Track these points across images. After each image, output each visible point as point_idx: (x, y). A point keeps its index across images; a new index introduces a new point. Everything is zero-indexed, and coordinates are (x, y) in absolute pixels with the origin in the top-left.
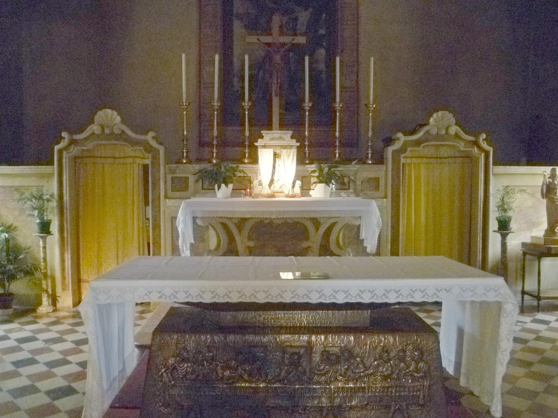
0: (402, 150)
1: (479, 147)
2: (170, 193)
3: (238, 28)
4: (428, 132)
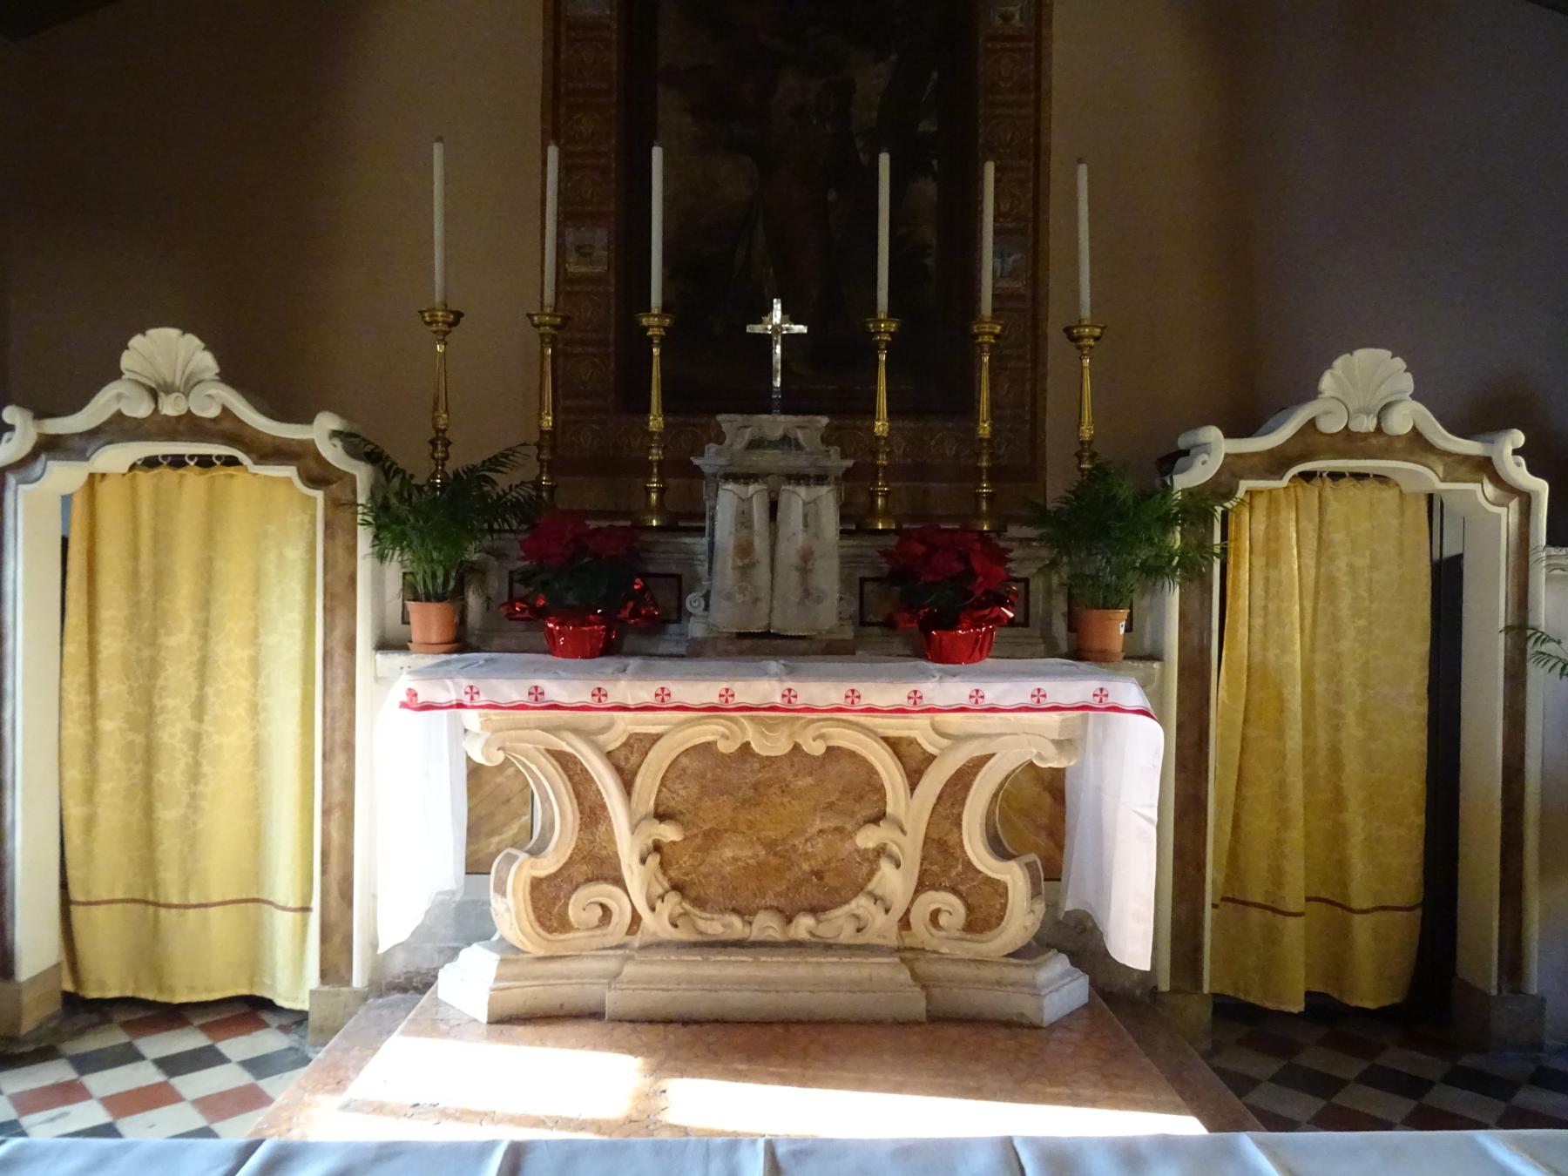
1: (1497, 480)
4: (1312, 423)
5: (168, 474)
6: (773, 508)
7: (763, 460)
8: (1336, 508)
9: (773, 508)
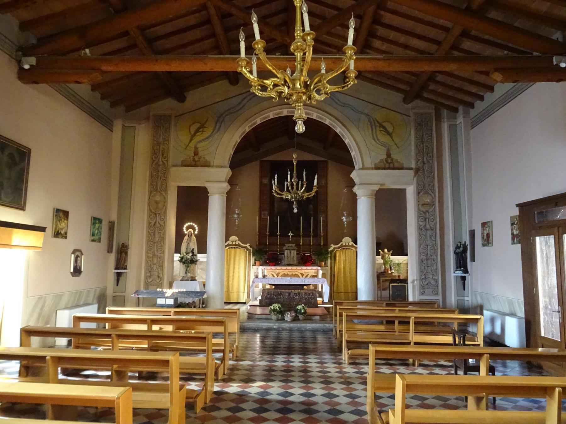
4: (342, 244)
5: (231, 249)
6: (290, 253)
7: (289, 248)
8: (347, 252)
9: (290, 253)
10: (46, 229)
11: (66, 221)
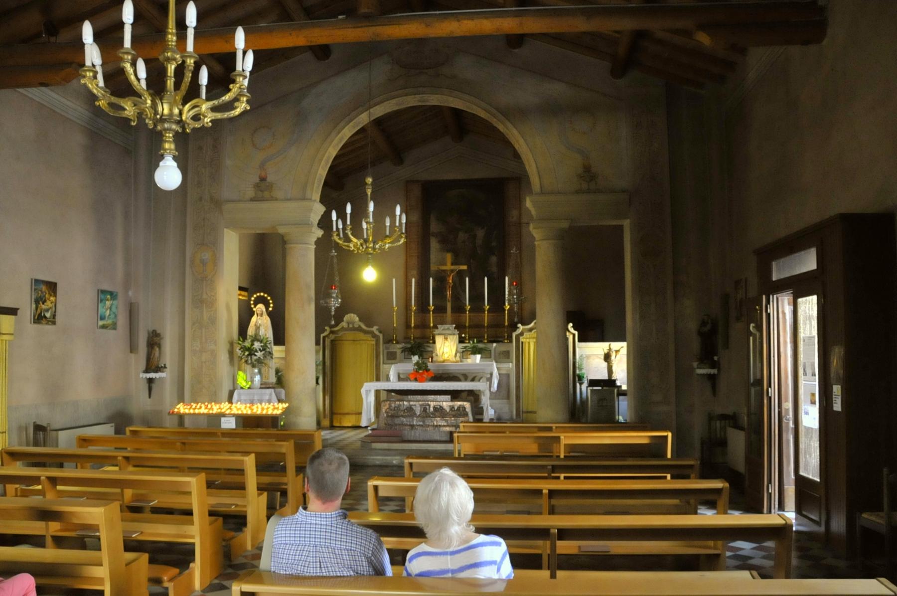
0: (522, 334)
2: (386, 361)
3: (434, 244)
10: (19, 311)
11: (52, 299)
